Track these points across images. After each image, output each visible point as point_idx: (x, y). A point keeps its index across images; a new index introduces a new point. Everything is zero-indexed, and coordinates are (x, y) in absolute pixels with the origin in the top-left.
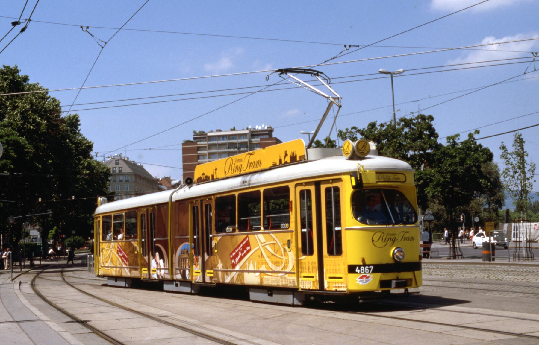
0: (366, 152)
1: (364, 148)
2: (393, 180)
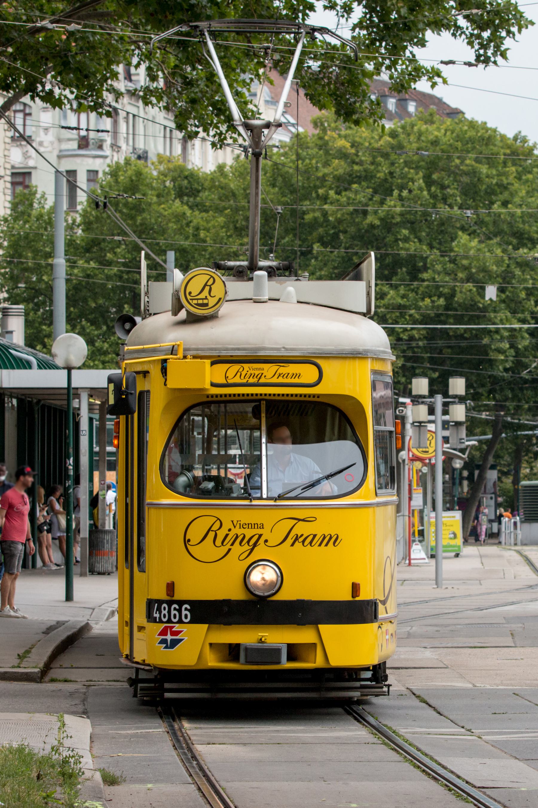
0: (212, 302)
1: (206, 293)
2: (275, 380)
